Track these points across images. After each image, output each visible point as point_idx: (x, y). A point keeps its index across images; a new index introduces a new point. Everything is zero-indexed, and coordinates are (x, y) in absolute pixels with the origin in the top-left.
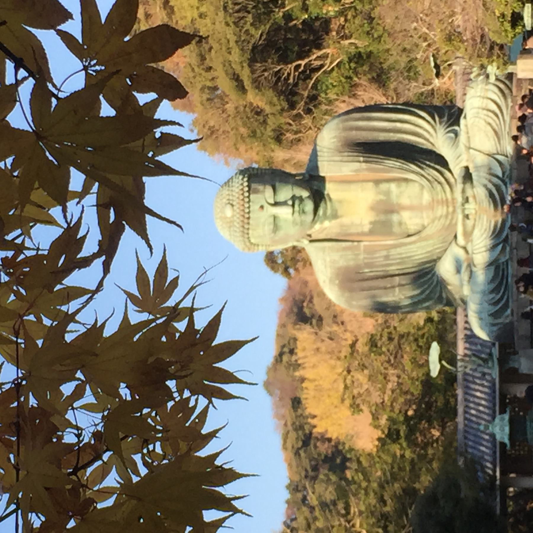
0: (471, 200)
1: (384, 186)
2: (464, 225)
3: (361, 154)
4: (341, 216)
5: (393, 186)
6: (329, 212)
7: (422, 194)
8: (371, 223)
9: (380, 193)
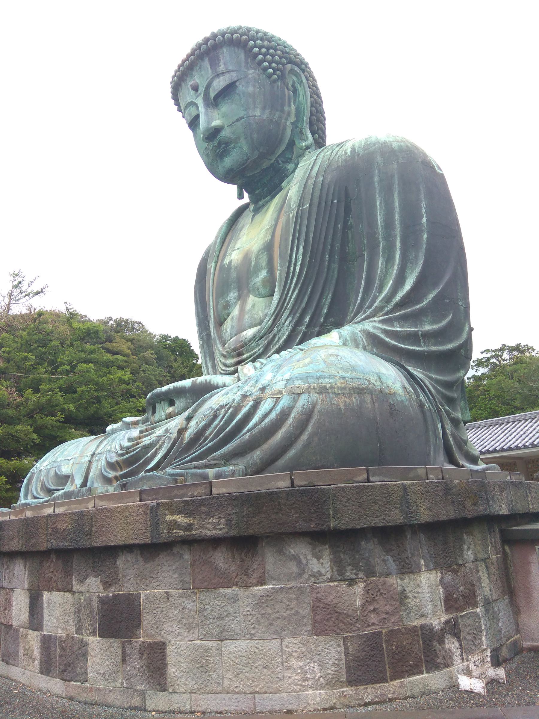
0: (171, 409)
3: (316, 201)
4: (252, 222)
5: (263, 274)
6: (261, 203)
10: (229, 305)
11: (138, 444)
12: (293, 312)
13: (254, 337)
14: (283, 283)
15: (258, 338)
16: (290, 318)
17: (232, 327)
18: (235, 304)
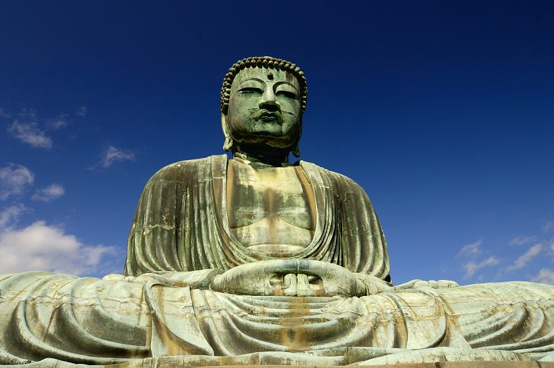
1: (301, 202)
2: (258, 275)
5: (303, 210)
7: (295, 244)
8: (250, 188)
9: (290, 197)
10: (254, 217)
11: (299, 314)
12: (329, 248)
13: (301, 253)
14: (323, 225)
15: (304, 256)
16: (328, 253)
17: (260, 234)
18: (261, 219)
